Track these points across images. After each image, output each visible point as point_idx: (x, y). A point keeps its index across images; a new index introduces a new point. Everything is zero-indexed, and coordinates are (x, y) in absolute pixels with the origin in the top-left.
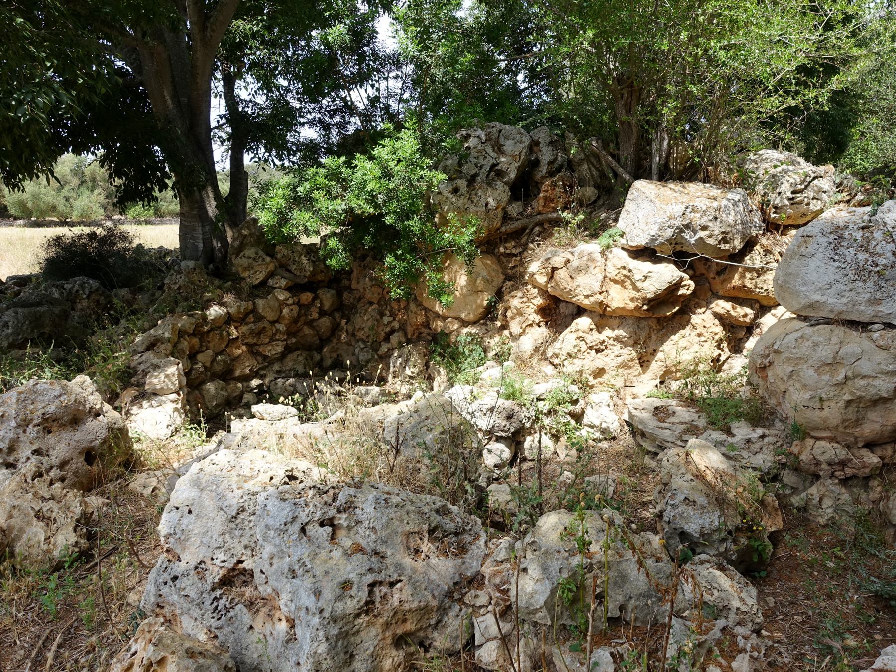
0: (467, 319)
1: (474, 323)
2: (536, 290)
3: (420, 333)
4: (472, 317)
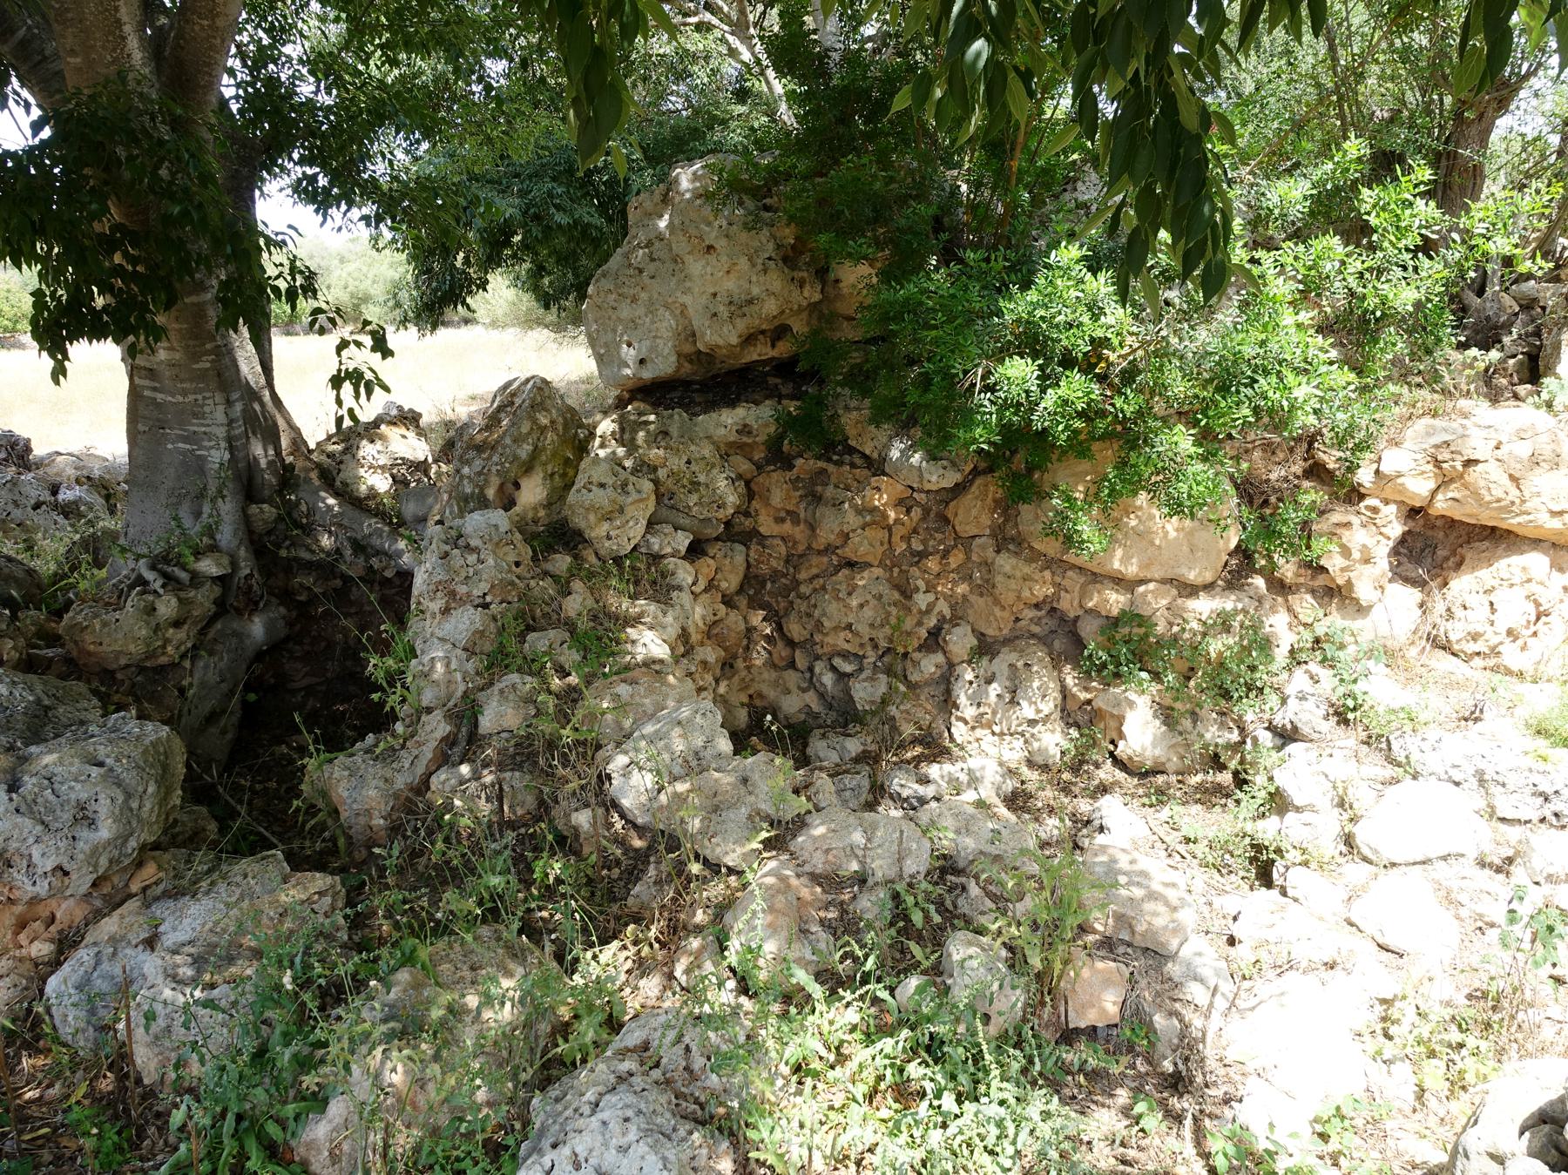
0: (1199, 581)
1: (1209, 587)
2: (1393, 508)
3: (1017, 620)
4: (1209, 577)
